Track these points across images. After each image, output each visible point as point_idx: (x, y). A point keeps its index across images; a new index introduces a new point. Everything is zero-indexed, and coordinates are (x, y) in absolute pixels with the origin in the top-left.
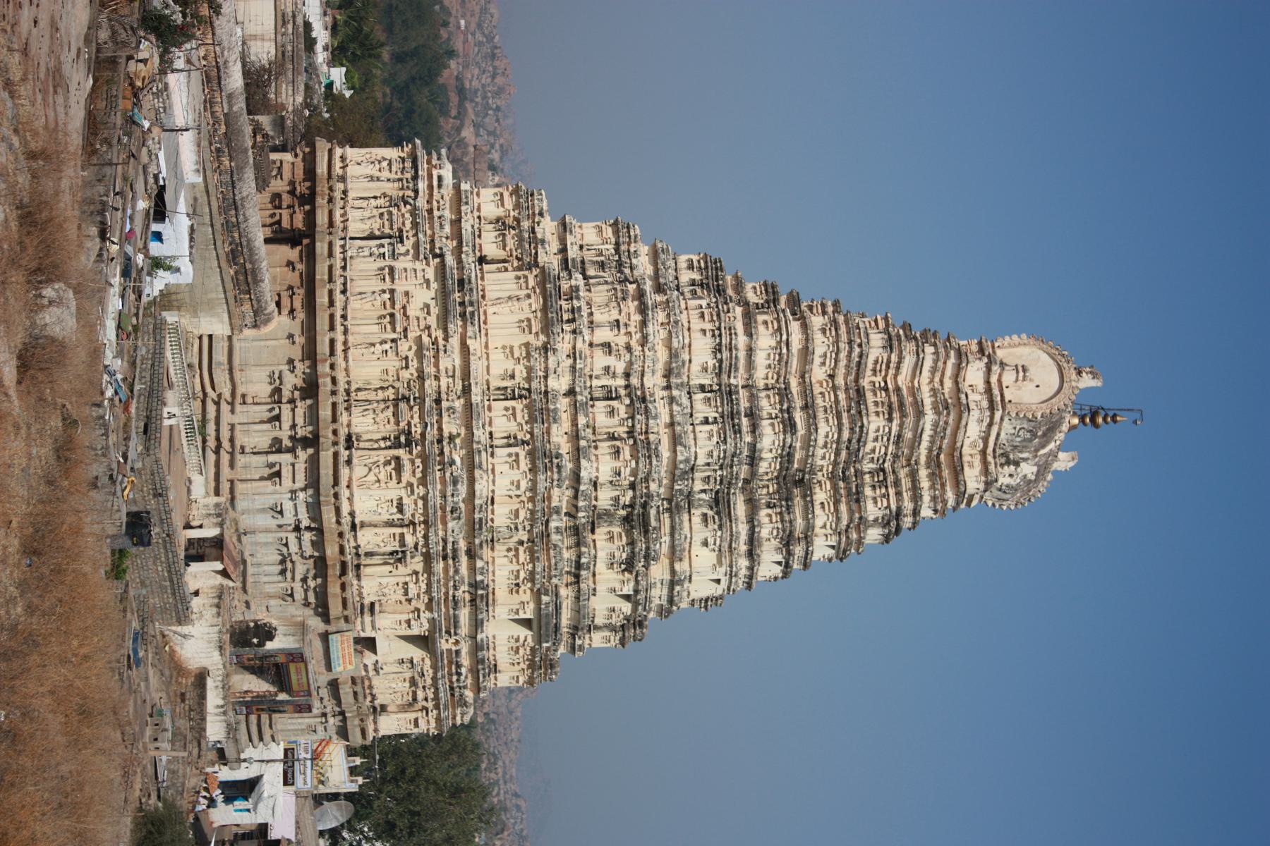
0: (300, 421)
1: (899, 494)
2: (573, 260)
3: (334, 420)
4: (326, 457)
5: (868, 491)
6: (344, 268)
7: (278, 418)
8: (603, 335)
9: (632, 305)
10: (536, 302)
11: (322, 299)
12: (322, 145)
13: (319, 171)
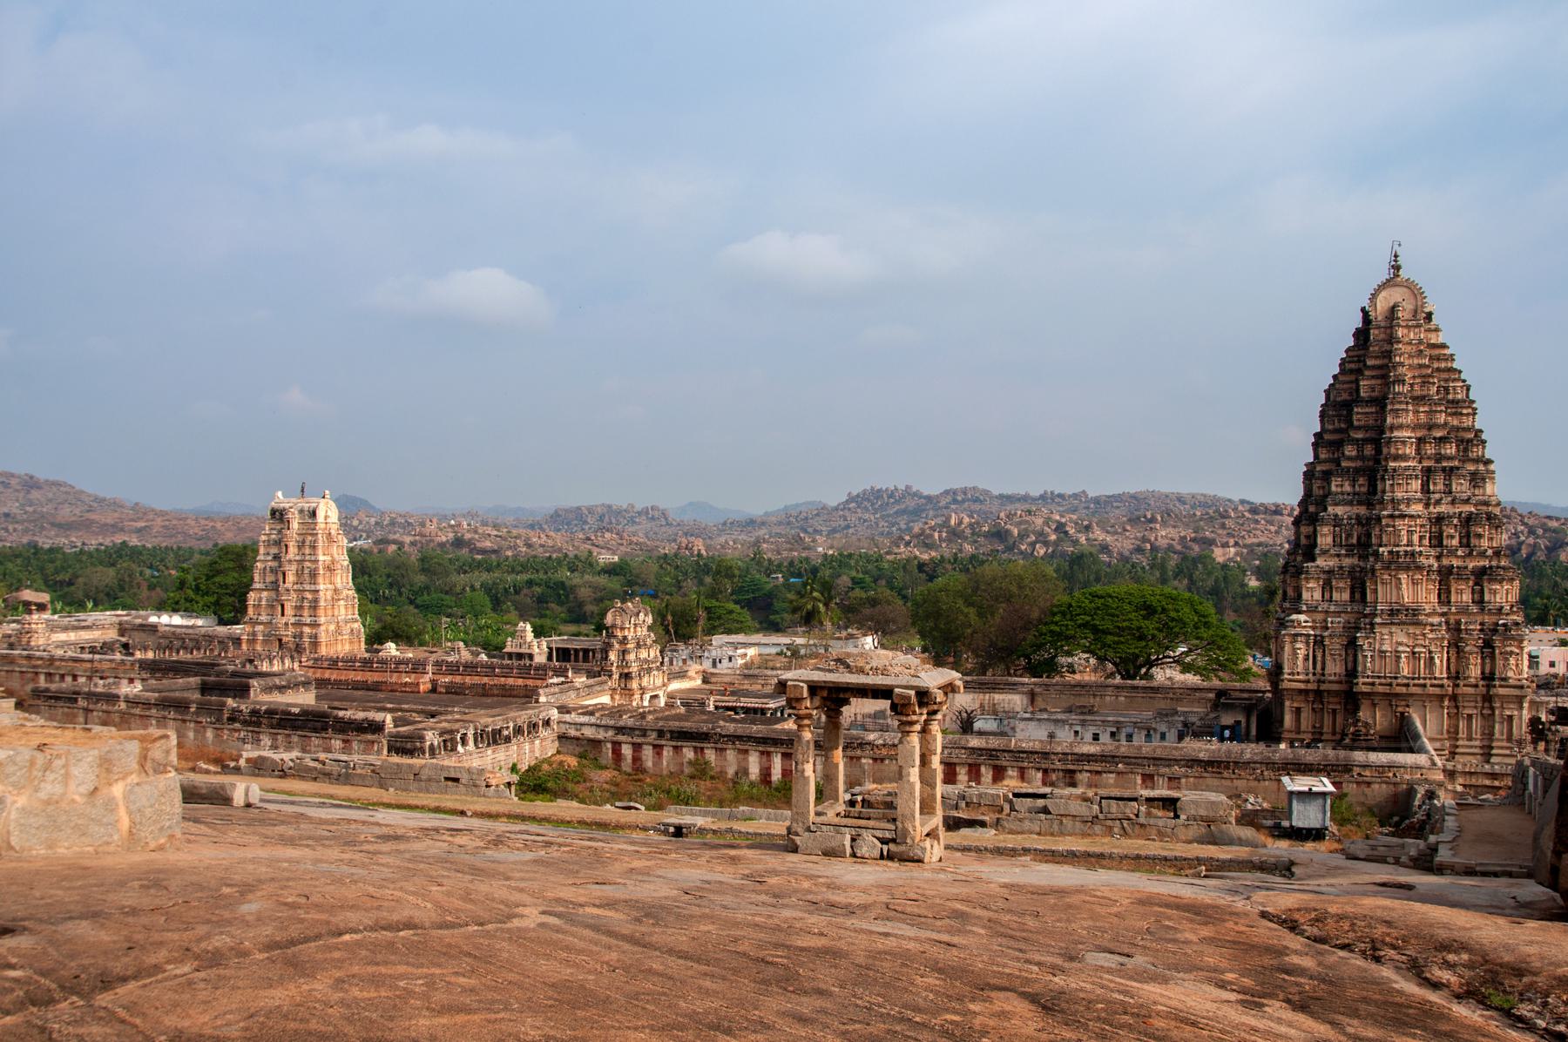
1: (1454, 380)
3: (1476, 686)
4: (1502, 691)
5: (1450, 397)
7: (1470, 716)
8: (1416, 538)
9: (1398, 522)
10: (1403, 576)
11: (1404, 690)
12: (1285, 685)
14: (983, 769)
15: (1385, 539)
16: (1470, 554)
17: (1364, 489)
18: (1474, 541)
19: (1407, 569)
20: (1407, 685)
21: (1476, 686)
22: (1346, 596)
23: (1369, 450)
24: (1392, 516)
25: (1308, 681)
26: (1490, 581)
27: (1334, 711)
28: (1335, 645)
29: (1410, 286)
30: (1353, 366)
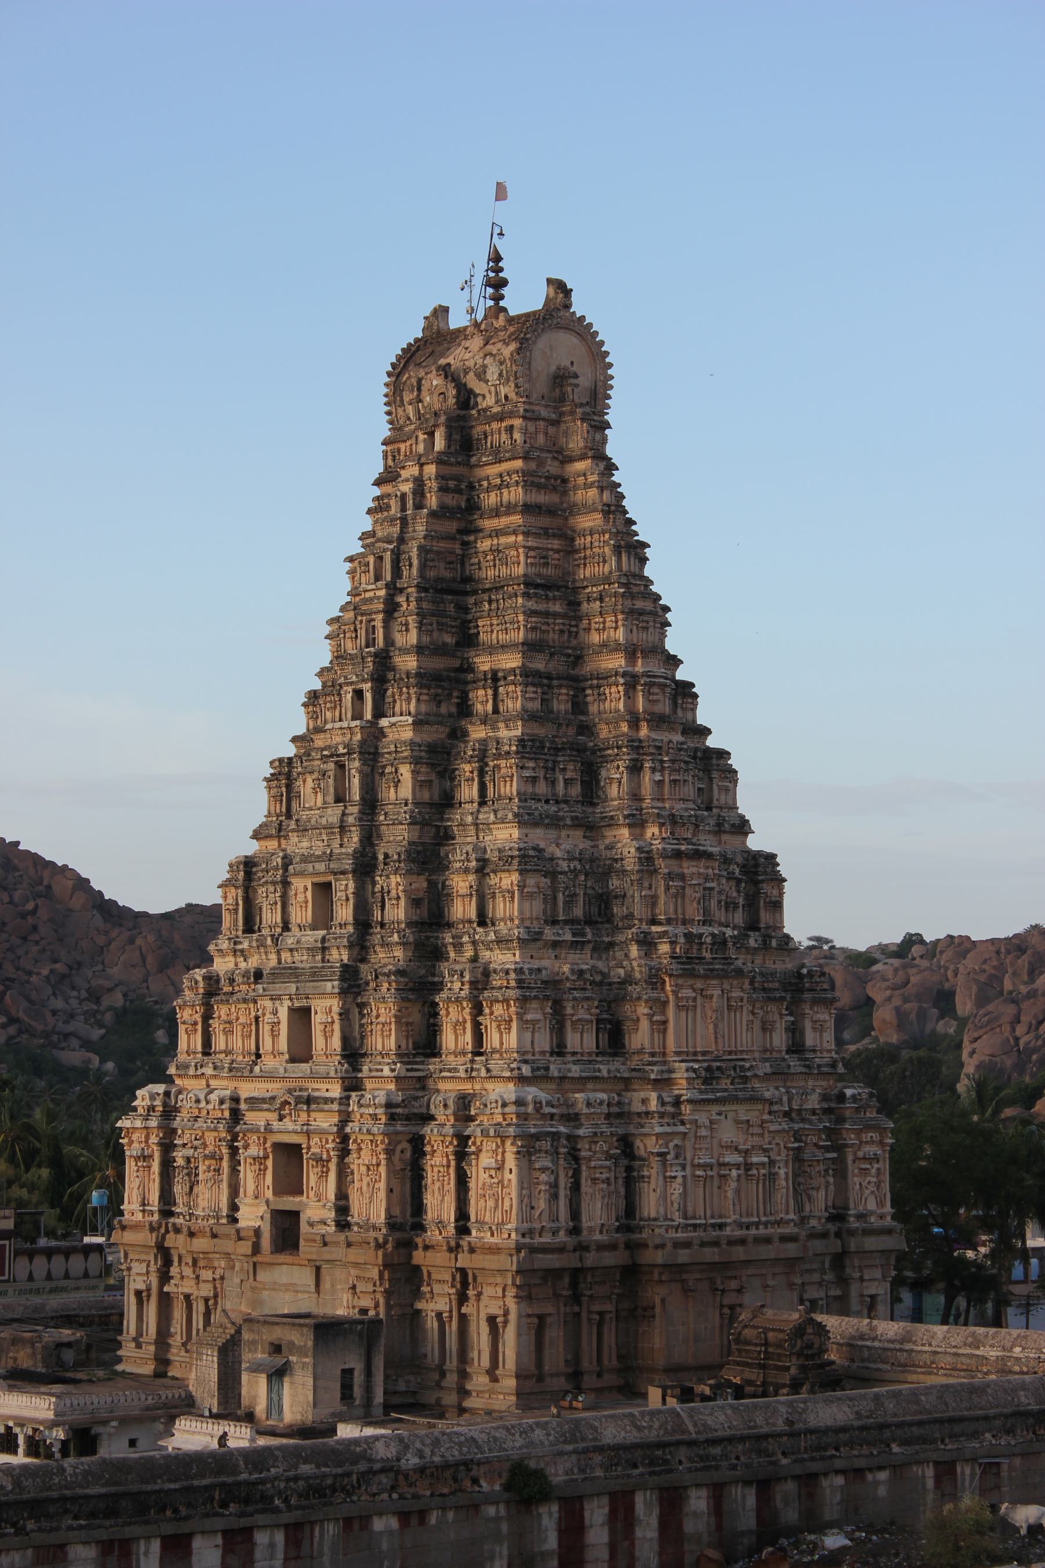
0: (816, 1277)
2: (574, 935)
3: (824, 1235)
6: (695, 1226)
9: (689, 868)
11: (739, 1253)
13: (557, 1265)
14: (639, 1499)
15: (664, 907)
16: (765, 945)
17: (576, 790)
18: (765, 917)
19: (723, 975)
20: (742, 1242)
21: (824, 1235)
22: (589, 1042)
23: (561, 704)
24: (678, 855)
25: (561, 1250)
26: (815, 1002)
27: (601, 1314)
28: (598, 1160)
29: (583, 331)
30: (450, 500)
